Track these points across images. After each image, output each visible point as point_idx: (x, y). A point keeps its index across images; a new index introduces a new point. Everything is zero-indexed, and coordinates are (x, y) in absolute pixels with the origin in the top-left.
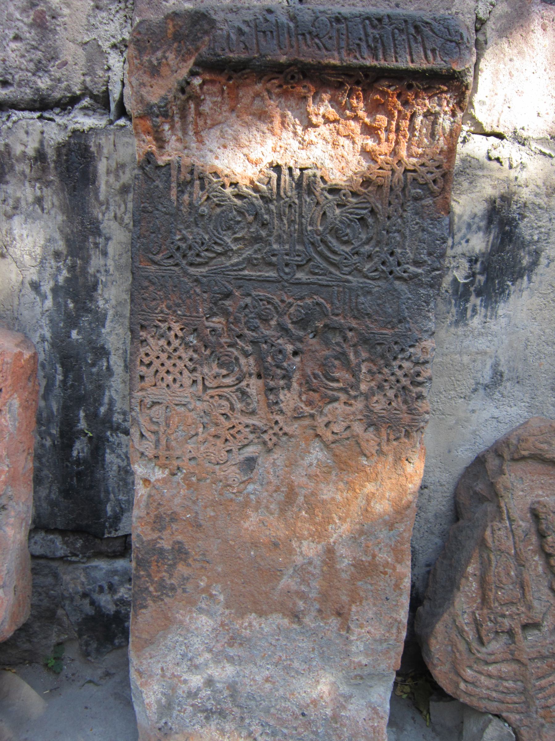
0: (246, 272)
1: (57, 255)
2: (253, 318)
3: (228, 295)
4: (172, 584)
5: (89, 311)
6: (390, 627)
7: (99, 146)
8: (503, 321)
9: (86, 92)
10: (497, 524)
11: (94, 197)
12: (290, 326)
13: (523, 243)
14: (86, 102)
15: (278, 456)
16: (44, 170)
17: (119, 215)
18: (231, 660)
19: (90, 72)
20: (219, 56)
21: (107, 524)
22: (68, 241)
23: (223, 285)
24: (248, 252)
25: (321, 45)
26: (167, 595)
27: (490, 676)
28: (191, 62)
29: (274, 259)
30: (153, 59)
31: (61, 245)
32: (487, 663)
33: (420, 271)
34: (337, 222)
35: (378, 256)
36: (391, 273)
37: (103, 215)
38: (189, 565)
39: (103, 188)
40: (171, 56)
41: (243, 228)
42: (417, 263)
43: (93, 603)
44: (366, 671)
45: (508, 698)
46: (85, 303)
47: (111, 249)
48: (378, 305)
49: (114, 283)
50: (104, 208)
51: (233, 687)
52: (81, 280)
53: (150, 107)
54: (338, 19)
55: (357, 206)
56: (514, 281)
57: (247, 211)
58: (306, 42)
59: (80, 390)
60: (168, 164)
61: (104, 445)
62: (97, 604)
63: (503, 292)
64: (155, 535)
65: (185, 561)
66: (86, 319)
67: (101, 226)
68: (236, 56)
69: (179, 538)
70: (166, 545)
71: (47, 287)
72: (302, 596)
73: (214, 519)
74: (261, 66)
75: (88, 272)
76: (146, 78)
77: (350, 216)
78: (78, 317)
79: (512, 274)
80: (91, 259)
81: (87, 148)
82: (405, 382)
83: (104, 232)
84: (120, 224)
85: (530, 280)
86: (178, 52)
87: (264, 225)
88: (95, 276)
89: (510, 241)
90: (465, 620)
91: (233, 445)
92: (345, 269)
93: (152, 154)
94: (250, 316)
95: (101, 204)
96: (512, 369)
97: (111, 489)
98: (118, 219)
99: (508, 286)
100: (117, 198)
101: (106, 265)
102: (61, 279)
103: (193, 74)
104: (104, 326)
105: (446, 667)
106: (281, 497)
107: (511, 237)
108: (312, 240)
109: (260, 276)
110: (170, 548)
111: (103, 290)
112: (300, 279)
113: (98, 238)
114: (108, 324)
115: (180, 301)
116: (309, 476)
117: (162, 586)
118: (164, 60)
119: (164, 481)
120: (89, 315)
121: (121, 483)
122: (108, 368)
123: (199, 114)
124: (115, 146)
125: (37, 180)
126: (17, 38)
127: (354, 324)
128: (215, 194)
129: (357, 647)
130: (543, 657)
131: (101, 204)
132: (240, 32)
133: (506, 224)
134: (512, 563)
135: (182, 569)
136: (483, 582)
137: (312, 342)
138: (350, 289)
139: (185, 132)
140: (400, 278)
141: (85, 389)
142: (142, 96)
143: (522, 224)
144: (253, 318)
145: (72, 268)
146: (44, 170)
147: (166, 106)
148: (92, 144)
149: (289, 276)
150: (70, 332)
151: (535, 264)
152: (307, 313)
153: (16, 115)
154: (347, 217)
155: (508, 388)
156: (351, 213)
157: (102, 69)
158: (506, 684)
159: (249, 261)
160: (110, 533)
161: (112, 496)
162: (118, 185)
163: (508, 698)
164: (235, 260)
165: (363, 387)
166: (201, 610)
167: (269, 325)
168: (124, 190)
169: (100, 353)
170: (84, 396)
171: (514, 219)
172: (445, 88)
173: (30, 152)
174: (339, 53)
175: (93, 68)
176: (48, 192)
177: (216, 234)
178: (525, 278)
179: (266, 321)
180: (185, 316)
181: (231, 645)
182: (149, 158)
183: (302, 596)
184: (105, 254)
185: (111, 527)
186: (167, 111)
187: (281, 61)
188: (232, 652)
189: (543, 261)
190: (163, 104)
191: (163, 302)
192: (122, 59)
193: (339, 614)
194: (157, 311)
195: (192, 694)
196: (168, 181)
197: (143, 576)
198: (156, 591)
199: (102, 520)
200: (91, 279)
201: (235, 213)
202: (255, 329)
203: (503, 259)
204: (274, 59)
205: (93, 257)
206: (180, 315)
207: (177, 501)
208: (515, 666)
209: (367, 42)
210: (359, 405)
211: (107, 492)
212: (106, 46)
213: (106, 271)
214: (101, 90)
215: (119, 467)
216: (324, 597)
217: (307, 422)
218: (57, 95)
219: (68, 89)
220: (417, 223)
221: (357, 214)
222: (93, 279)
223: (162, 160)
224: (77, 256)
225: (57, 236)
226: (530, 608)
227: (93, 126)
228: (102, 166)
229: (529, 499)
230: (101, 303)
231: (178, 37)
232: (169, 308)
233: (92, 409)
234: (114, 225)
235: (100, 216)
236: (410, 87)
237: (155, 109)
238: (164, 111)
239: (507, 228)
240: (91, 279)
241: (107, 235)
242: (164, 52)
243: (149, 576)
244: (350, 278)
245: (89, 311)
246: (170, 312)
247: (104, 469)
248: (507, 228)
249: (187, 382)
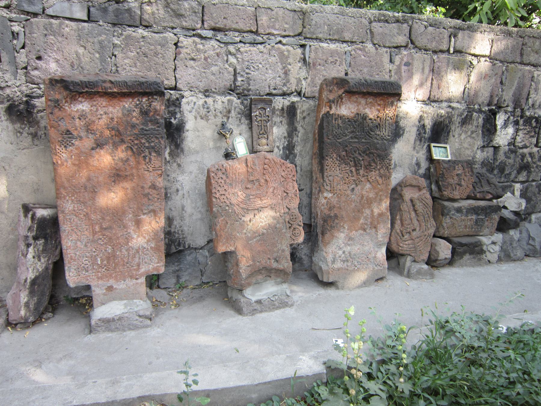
1: (285, 137)
3: (347, 146)
5: (292, 154)
6: (387, 229)
7: (298, 106)
8: (396, 149)
9: (296, 91)
10: (403, 204)
14: (295, 94)
15: (359, 187)
16: (283, 113)
18: (349, 245)
19: (297, 85)
22: (288, 133)
24: (351, 135)
27: (406, 245)
28: (342, 90)
31: (286, 135)
32: (405, 241)
39: (298, 118)
40: (335, 88)
42: (389, 136)
44: (382, 242)
45: (412, 249)
47: (300, 135)
51: (350, 253)
53: (330, 100)
54: (376, 82)
60: (333, 114)
64: (329, 212)
66: (291, 156)
69: (336, 212)
70: (332, 215)
71: (281, 147)
72: (366, 224)
73: (344, 206)
76: (329, 93)
78: (289, 155)
81: (295, 106)
82: (388, 165)
86: (337, 87)
87: (355, 128)
90: (398, 231)
91: (349, 185)
96: (399, 163)
102: (285, 145)
103: (343, 93)
105: (395, 245)
106: (360, 198)
114: (297, 157)
116: (367, 192)
117: (331, 227)
119: (332, 197)
123: (341, 101)
125: (281, 116)
126: (279, 77)
127: (376, 152)
129: (380, 236)
130: (418, 238)
132: (355, 85)
134: (408, 214)
135: (336, 221)
136: (401, 220)
137: (366, 157)
139: (337, 106)
140: (386, 140)
145: (288, 141)
146: (283, 113)
151: (403, 133)
153: (277, 98)
159: (352, 138)
162: (302, 117)
163: (412, 249)
164: (348, 137)
165: (378, 167)
166: (341, 232)
168: (304, 118)
173: (280, 108)
176: (284, 119)
179: (355, 152)
181: (349, 241)
182: (328, 112)
183: (366, 224)
184: (298, 136)
188: (349, 243)
189: (405, 132)
193: (375, 228)
195: (340, 257)
196: (332, 118)
202: (353, 155)
207: (335, 202)
208: (412, 241)
210: (377, 172)
212: (302, 79)
216: (371, 223)
217: (366, 177)
218: (288, 92)
219: (291, 90)
223: (331, 113)
225: (285, 132)
226: (413, 225)
228: (298, 111)
229: (409, 197)
230: (296, 151)
231: (337, 84)
234: (301, 128)
243: (328, 224)
245: (292, 154)
249: (338, 169)
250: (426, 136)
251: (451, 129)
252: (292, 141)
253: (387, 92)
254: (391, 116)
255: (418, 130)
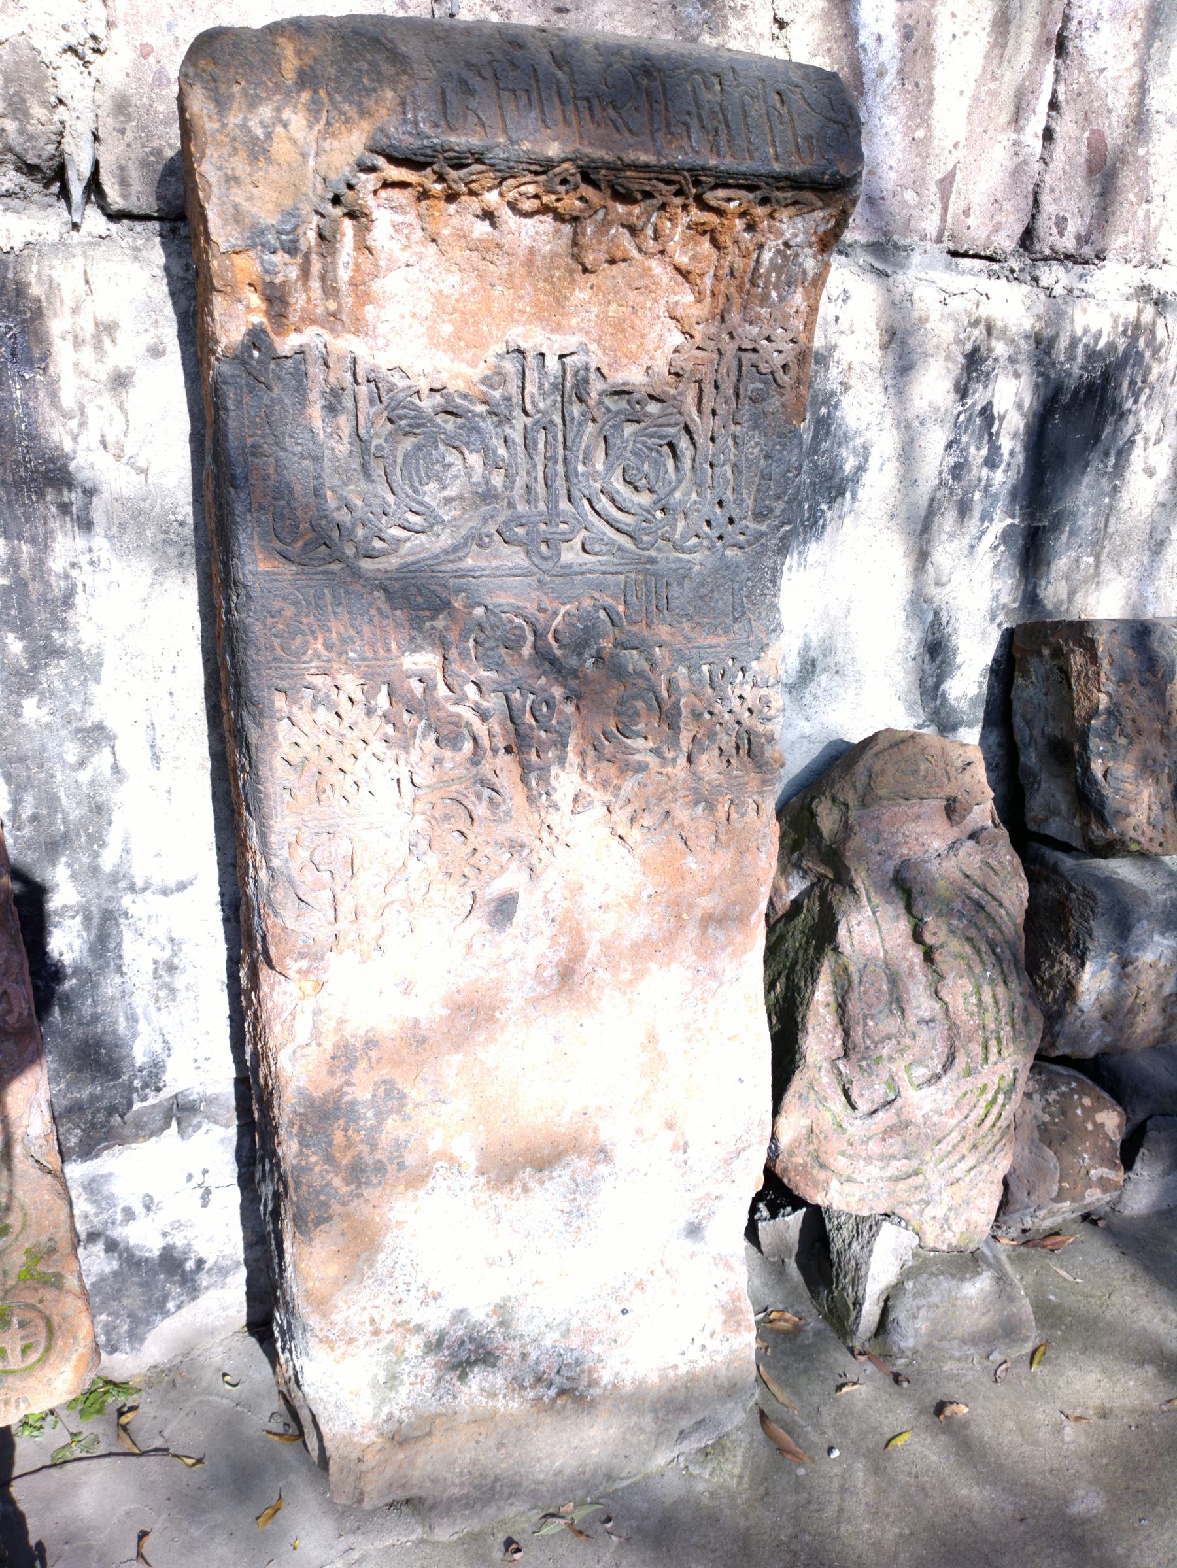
0: (470, 562)
2: (492, 649)
4: (380, 1161)
5: (59, 652)
7: (52, 287)
11: (47, 401)
12: (558, 652)
13: (845, 434)
17: (110, 440)
20: (428, 137)
21: (137, 1083)
23: (433, 592)
25: (619, 122)
26: (368, 1184)
29: (520, 531)
30: (251, 124)
33: (764, 528)
34: (628, 455)
35: (698, 511)
36: (720, 538)
37: (75, 438)
38: (406, 1118)
40: (297, 120)
41: (457, 477)
42: (760, 516)
43: (112, 1246)
46: (48, 637)
48: (702, 598)
49: (114, 586)
50: (73, 424)
52: (35, 589)
55: (660, 421)
56: (831, 502)
57: (467, 444)
58: (592, 116)
59: (52, 823)
61: (118, 925)
62: (122, 1246)
63: (816, 523)
65: (399, 1112)
67: (72, 467)
68: (463, 140)
74: (507, 160)
75: (50, 570)
77: (650, 441)
78: (35, 668)
79: (830, 489)
80: (54, 540)
83: (80, 476)
84: (118, 457)
85: (854, 497)
86: (314, 110)
88: (67, 576)
89: (828, 434)
92: (645, 538)
93: (264, 331)
94: (487, 645)
95: (67, 416)
97: (139, 1011)
98: (110, 446)
99: (823, 512)
100: (106, 399)
101: (90, 550)
104: (97, 681)
107: (829, 425)
108: (587, 492)
109: (496, 568)
110: (369, 1096)
111: (88, 604)
112: (570, 566)
113: (66, 492)
114: (105, 673)
115: (352, 632)
118: (279, 129)
120: (62, 663)
121: (162, 994)
122: (116, 769)
124: (87, 282)
128: (402, 412)
131: (67, 416)
133: (823, 404)
138: (655, 574)
141: (65, 821)
142: (236, 206)
143: (846, 401)
144: (492, 649)
147: (294, 229)
148: (32, 278)
149: (551, 564)
150: (19, 705)
151: (861, 468)
152: (586, 627)
154: (644, 444)
155: (823, 684)
156: (651, 436)
157: (44, 103)
158: (895, 1163)
160: (144, 1099)
161: (142, 1026)
162: (103, 372)
167: (521, 656)
169: (96, 741)
170: (65, 836)
171: (833, 394)
172: (820, 204)
174: (654, 140)
175: (23, 100)
177: (410, 492)
178: (848, 495)
180: (365, 659)
185: (146, 1085)
186: (295, 241)
187: (550, 153)
190: (288, 227)
191: (316, 639)
192: (92, 82)
194: (305, 658)
197: (316, 1164)
198: (348, 1184)
199: (125, 1077)
200: (58, 586)
201: (442, 447)
203: (817, 466)
204: (537, 149)
205: (59, 535)
206: (353, 660)
209: (700, 117)
211: (132, 1019)
213: (92, 563)
214: (45, 155)
215: (155, 962)
220: (757, 444)
221: (660, 437)
222: (62, 584)
223: (287, 344)
224: (20, 537)
227: (32, 239)
232: (329, 647)
233: (86, 859)
235: (68, 446)
236: (764, 201)
237: (271, 237)
238: (291, 241)
239: (823, 410)
240: (58, 586)
241: (88, 485)
242: (278, 110)
243: (329, 1159)
244: (652, 553)
245: (59, 652)
246: (333, 655)
247: (122, 974)
248: (823, 410)
250: (999, 476)
251: (1138, 428)
252: (39, 564)
253: (747, 165)
254: (777, 360)
255: (949, 446)
